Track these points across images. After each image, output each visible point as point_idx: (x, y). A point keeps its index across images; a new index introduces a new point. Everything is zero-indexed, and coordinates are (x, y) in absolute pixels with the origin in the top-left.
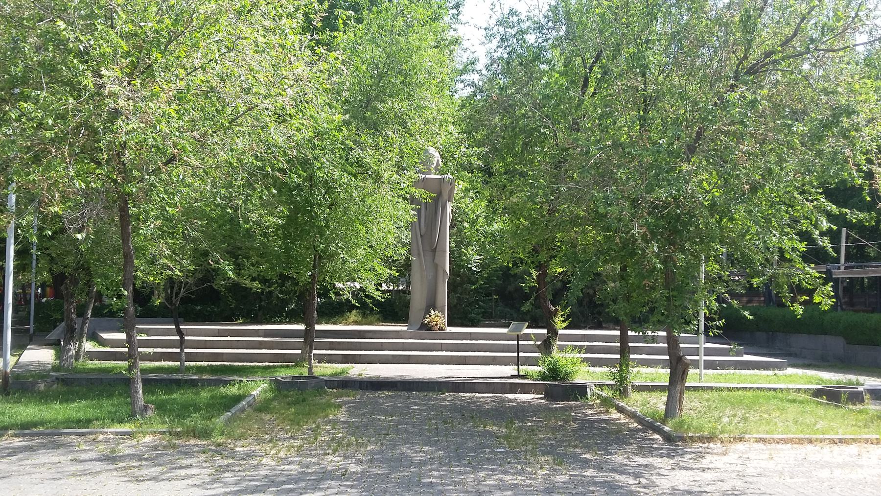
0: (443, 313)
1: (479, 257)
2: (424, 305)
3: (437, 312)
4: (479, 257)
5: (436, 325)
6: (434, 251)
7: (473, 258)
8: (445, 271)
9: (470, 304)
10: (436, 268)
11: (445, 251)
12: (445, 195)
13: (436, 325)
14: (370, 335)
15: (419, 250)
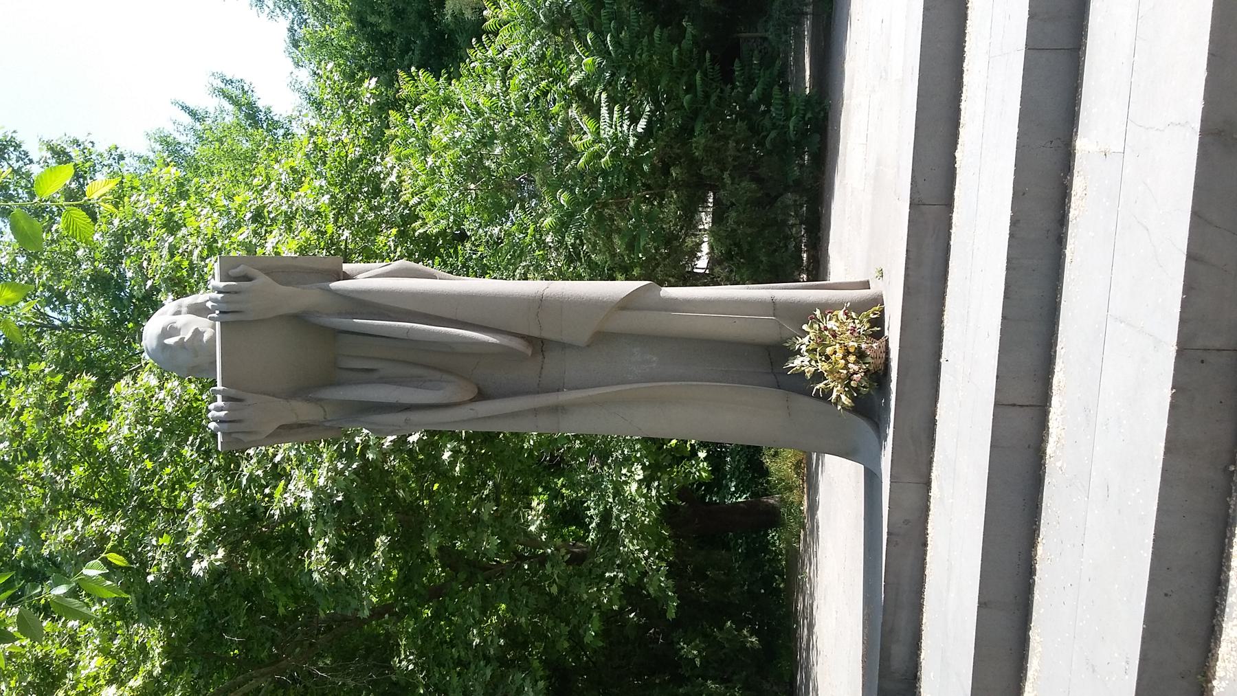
0: (803, 313)
1: (604, 111)
2: (772, 397)
3: (804, 343)
4: (604, 111)
5: (861, 355)
6: (539, 345)
7: (606, 131)
8: (626, 304)
9: (754, 129)
10: (608, 333)
11: (540, 303)
12: (303, 297)
13: (861, 355)
14: (899, 652)
15: (536, 411)
